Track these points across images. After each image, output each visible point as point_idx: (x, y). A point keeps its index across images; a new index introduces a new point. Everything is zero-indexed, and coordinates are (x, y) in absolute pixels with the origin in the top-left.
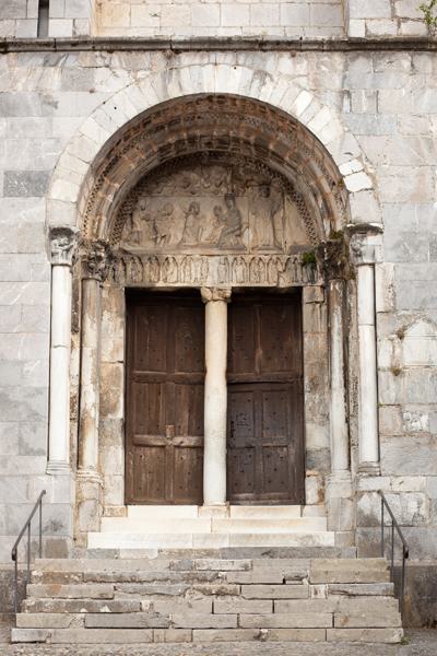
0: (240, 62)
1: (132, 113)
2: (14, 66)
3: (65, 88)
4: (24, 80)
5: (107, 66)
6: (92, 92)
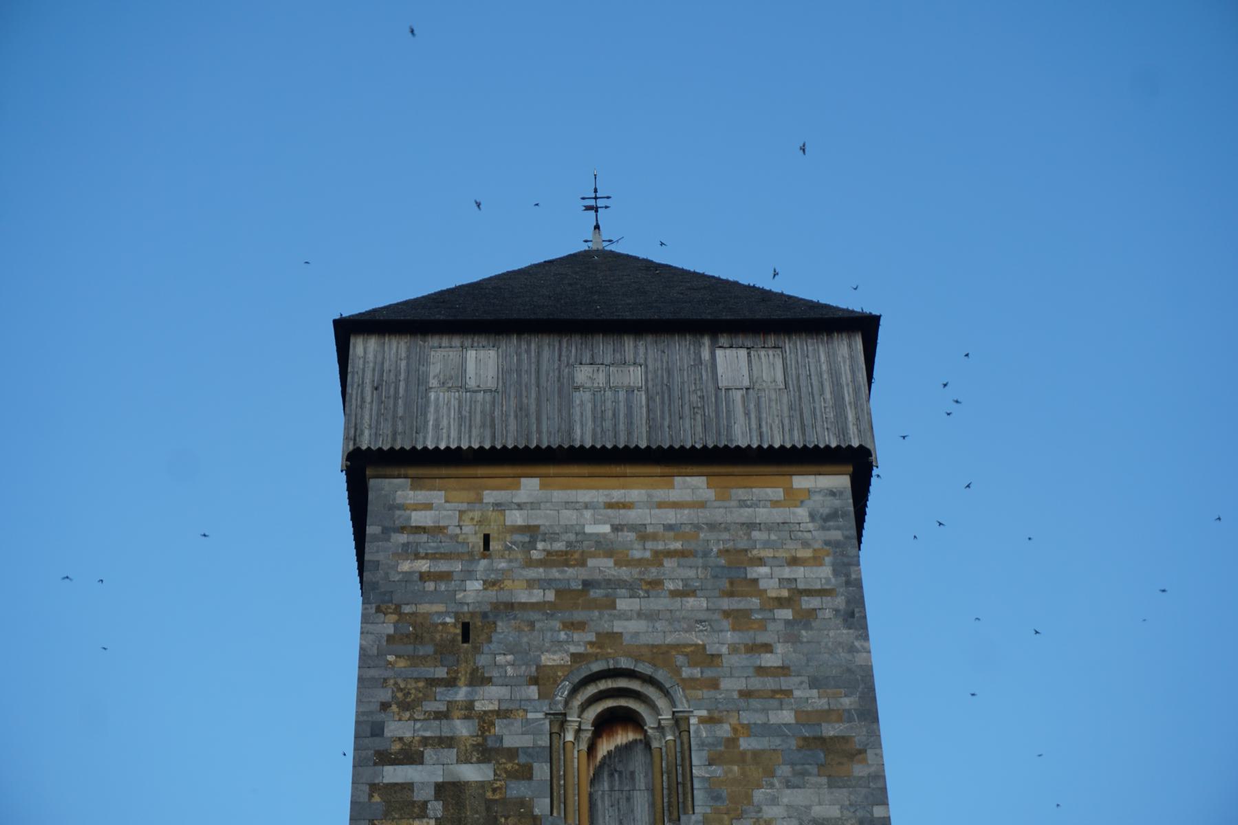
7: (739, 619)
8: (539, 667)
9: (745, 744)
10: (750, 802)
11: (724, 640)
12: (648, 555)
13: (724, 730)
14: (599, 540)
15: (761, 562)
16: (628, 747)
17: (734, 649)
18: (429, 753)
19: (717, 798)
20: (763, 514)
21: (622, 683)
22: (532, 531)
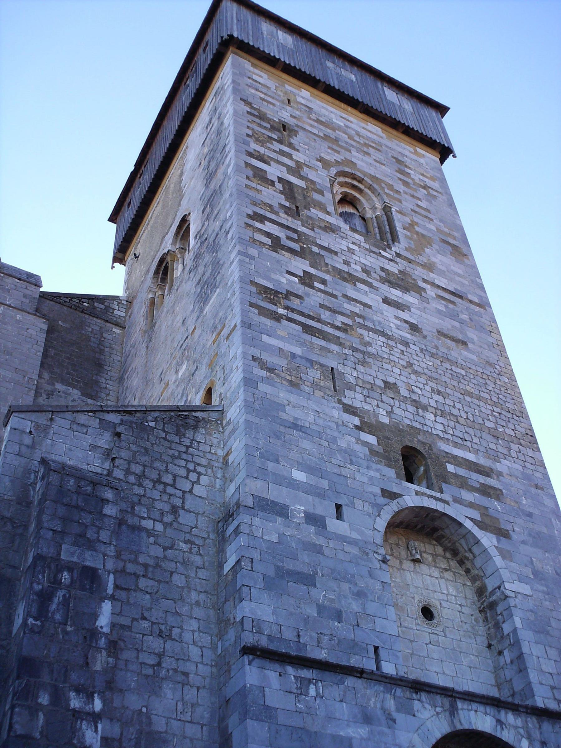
0: (488, 712)
1: (439, 736)
2: (367, 689)
3: (398, 710)
4: (373, 700)
5: (419, 700)
6: (414, 715)
7: (406, 184)
8: (320, 157)
9: (417, 229)
10: (424, 251)
11: (401, 187)
12: (362, 142)
13: (407, 220)
14: (340, 126)
15: (410, 168)
16: (352, 214)
17: (405, 193)
18: (272, 163)
19: (410, 243)
20: (407, 153)
21: (356, 183)
22: (310, 109)
